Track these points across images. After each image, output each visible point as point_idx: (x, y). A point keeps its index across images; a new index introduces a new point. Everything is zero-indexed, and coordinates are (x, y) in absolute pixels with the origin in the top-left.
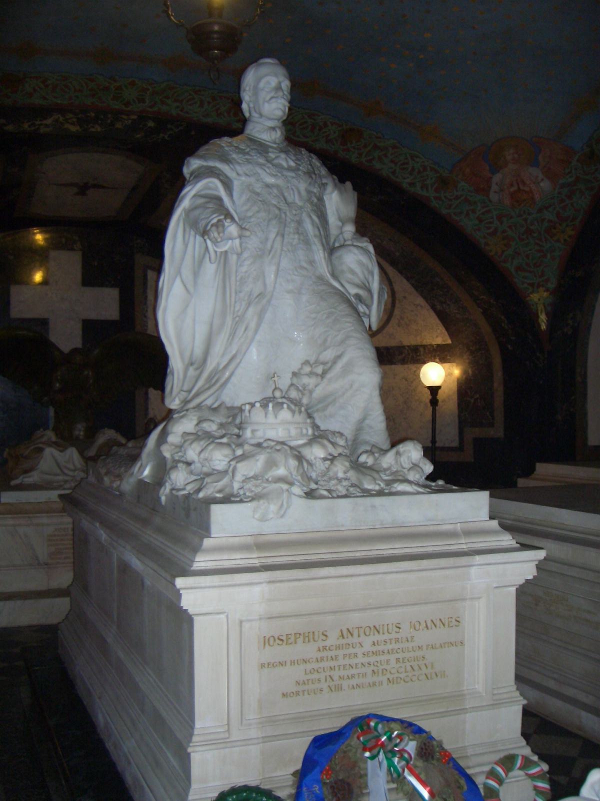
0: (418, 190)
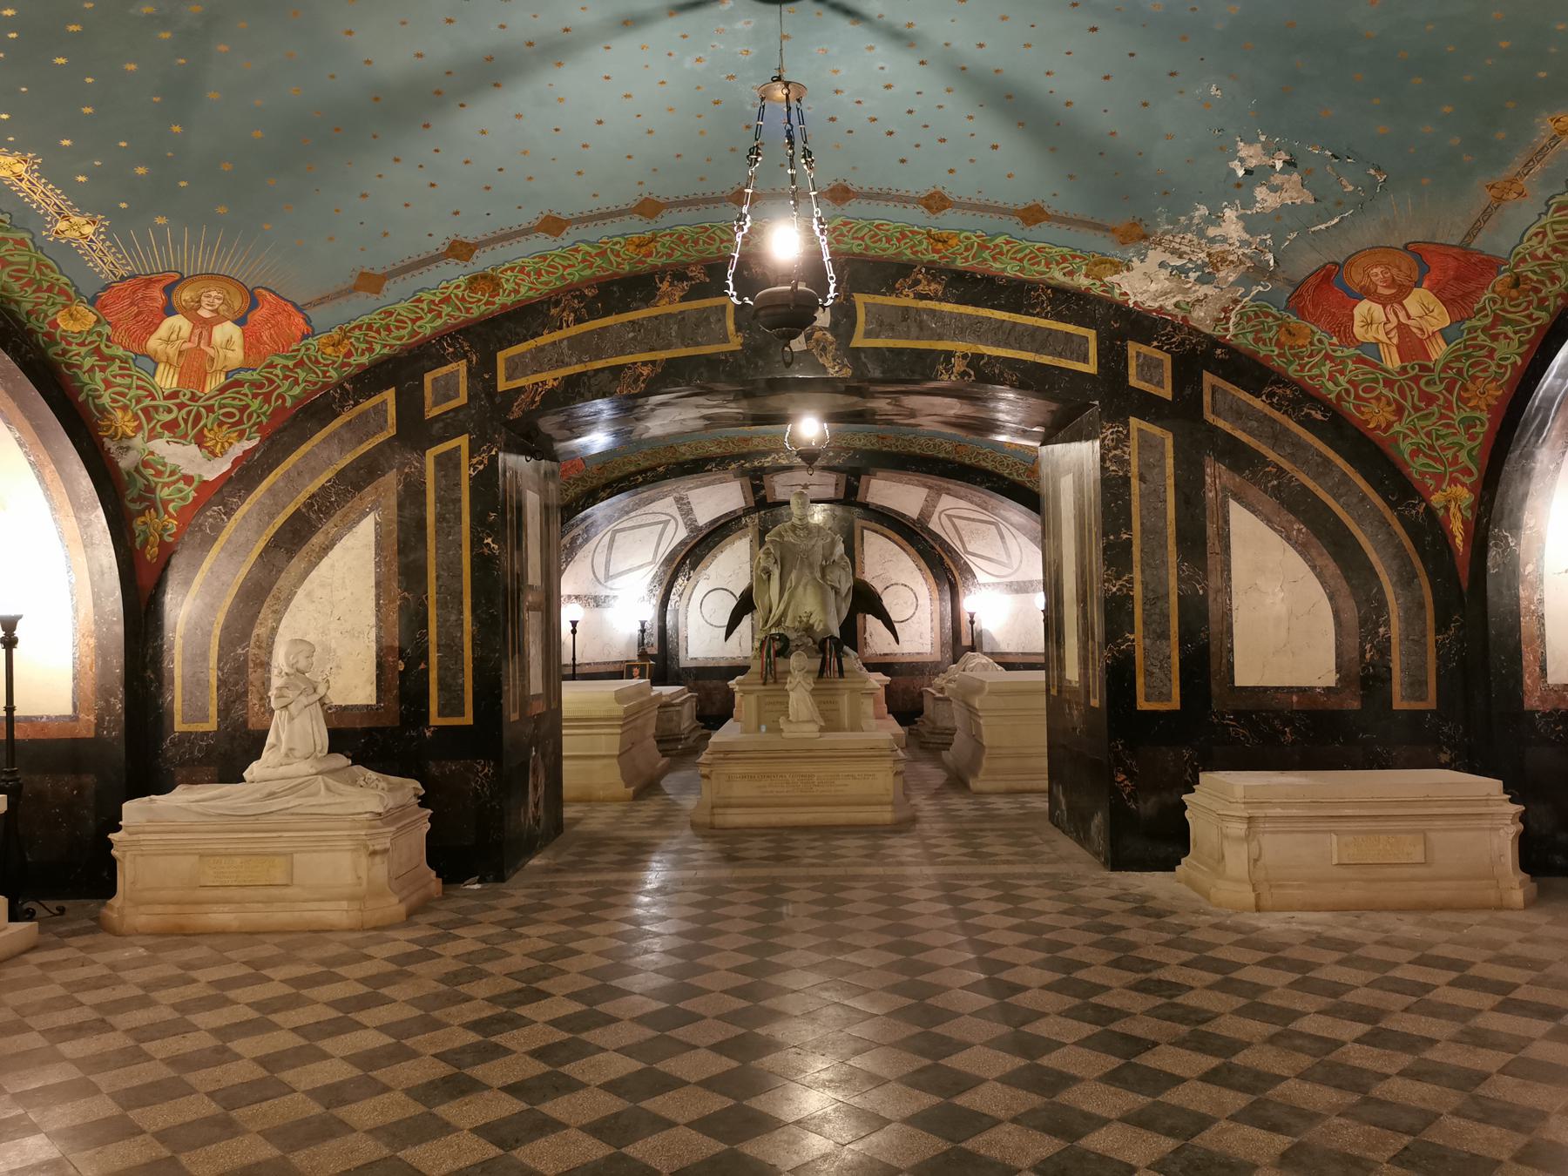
0: (1015, 476)
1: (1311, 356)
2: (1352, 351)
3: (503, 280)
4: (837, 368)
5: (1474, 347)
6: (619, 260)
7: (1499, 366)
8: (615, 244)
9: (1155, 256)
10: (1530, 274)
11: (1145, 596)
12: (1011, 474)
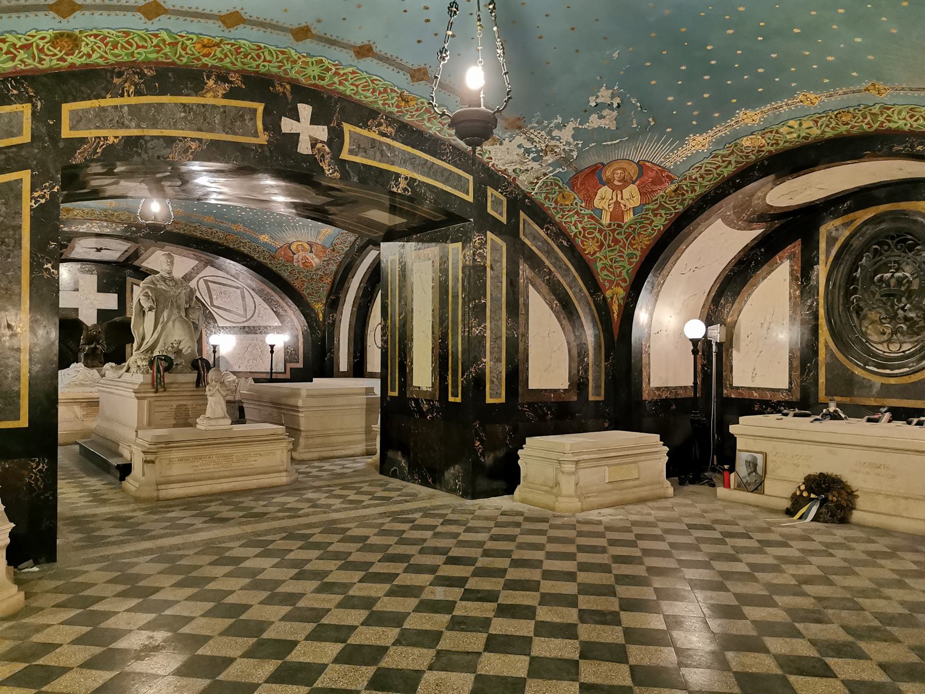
0: (261, 259)
1: (569, 211)
2: (590, 212)
3: (83, 43)
4: (331, 171)
5: (645, 218)
6: (183, 53)
7: (653, 229)
8: (189, 39)
9: (520, 139)
10: (684, 186)
11: (491, 337)
12: (259, 257)
